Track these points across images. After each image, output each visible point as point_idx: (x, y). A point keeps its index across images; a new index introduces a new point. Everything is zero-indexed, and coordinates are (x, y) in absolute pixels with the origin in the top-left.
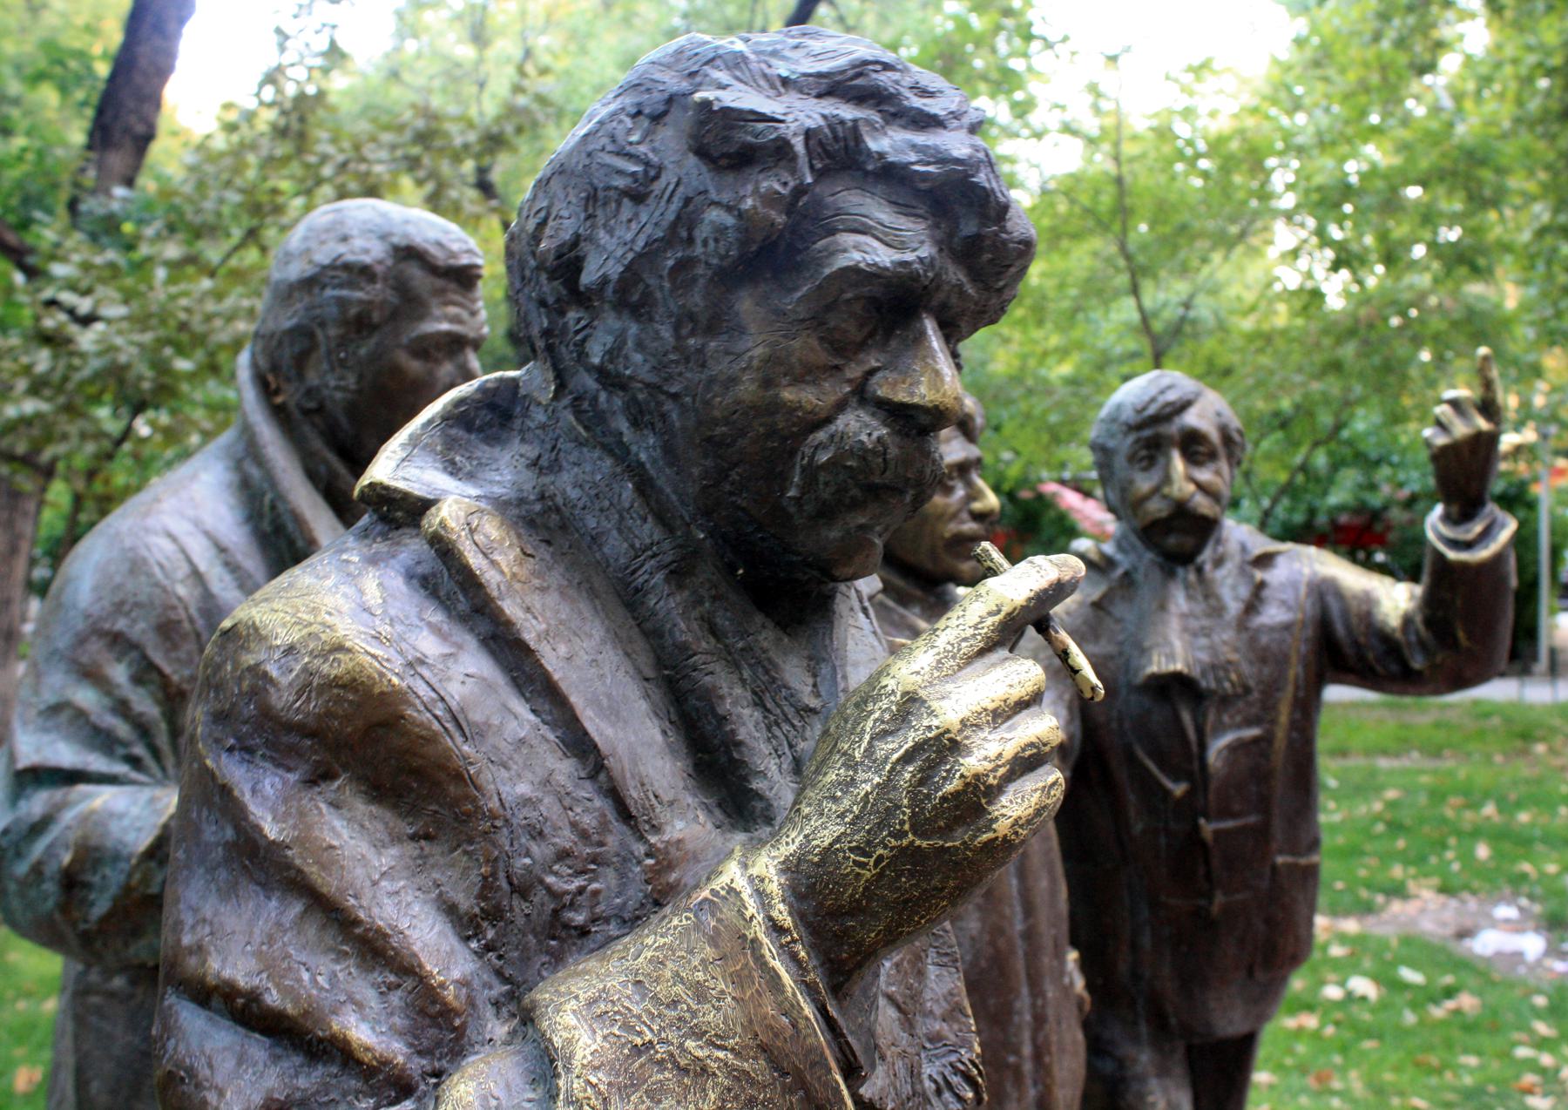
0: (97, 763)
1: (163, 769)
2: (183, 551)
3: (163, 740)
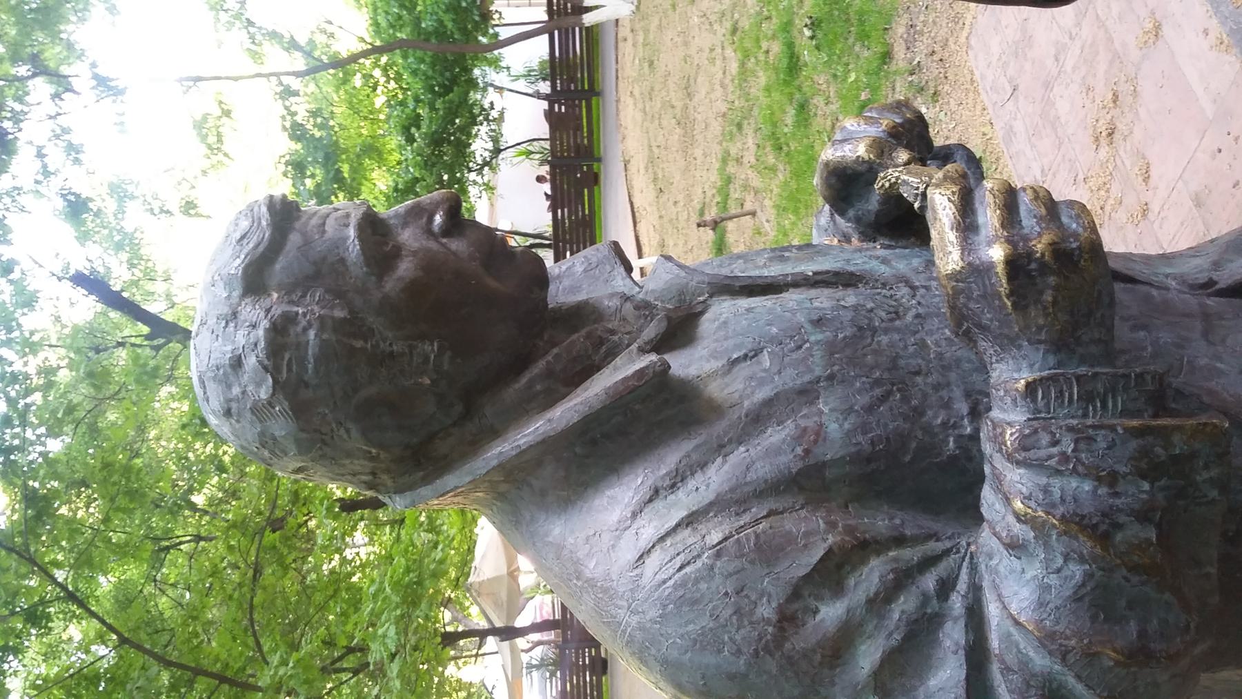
0: (953, 634)
1: (947, 552)
2: (662, 539)
3: (911, 554)
